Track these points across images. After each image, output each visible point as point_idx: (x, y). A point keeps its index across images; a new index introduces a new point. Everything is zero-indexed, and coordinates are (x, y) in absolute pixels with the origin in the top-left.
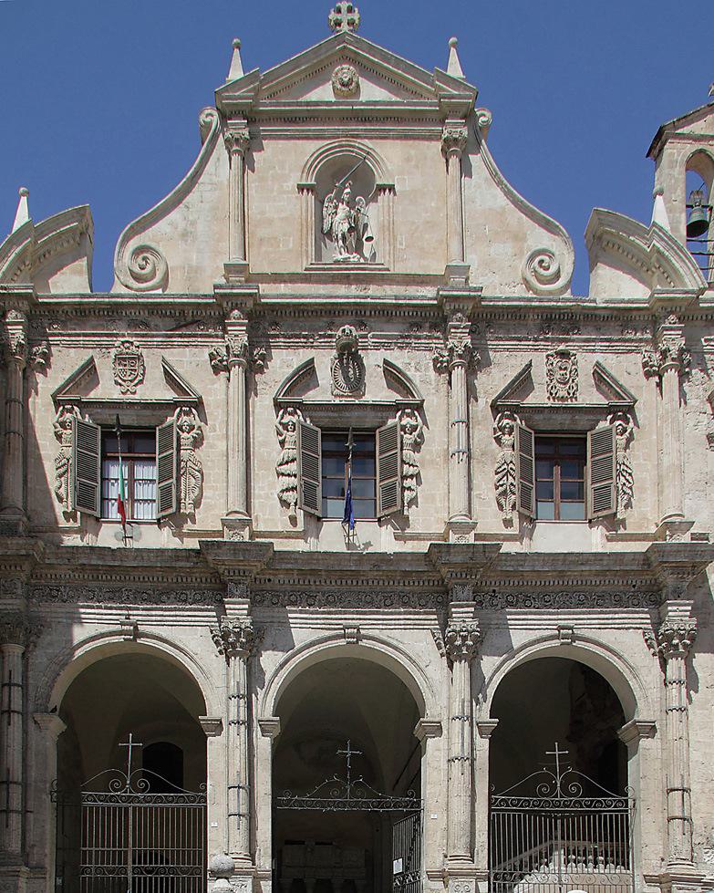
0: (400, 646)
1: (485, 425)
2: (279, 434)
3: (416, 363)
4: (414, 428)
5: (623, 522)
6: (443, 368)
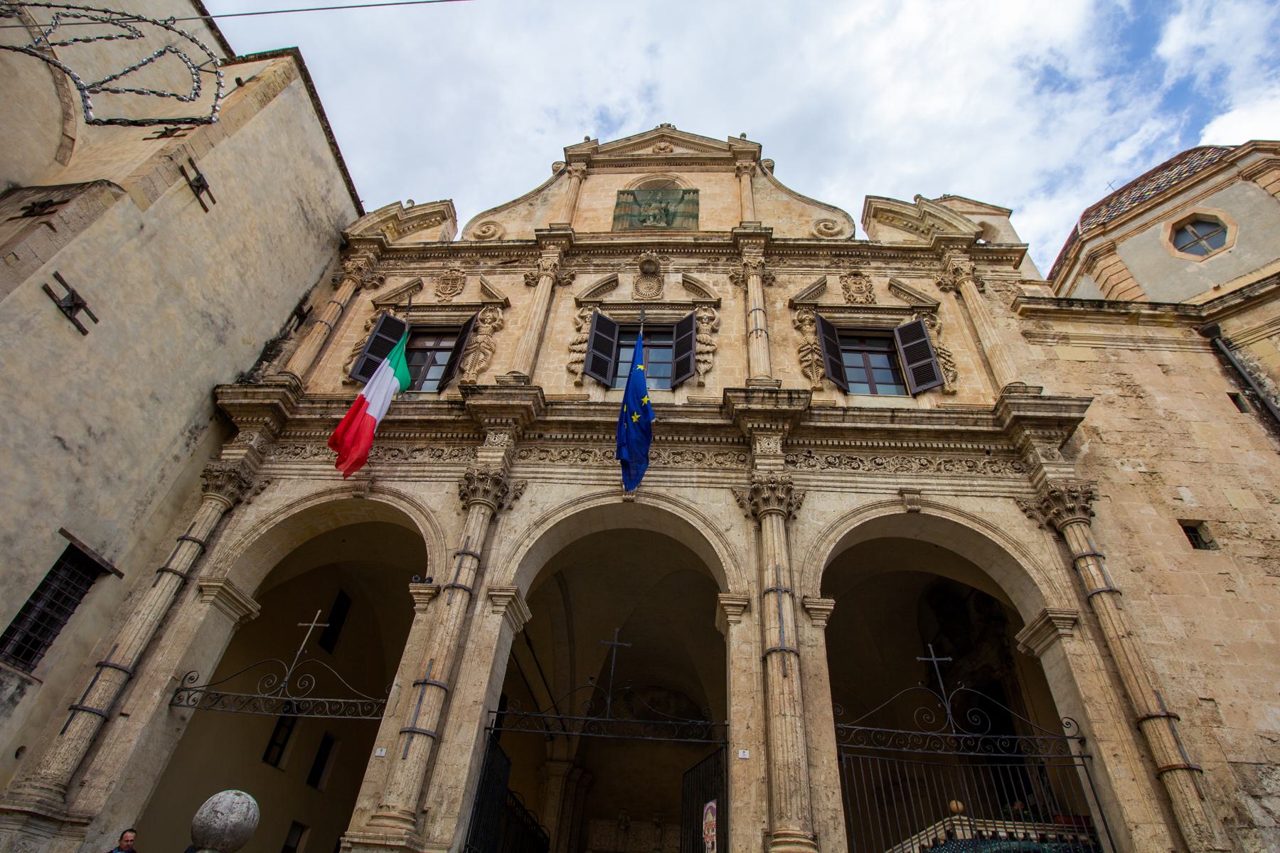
0: (693, 505)
1: (784, 324)
2: (577, 324)
3: (716, 281)
4: (712, 319)
5: (954, 393)
6: (740, 281)
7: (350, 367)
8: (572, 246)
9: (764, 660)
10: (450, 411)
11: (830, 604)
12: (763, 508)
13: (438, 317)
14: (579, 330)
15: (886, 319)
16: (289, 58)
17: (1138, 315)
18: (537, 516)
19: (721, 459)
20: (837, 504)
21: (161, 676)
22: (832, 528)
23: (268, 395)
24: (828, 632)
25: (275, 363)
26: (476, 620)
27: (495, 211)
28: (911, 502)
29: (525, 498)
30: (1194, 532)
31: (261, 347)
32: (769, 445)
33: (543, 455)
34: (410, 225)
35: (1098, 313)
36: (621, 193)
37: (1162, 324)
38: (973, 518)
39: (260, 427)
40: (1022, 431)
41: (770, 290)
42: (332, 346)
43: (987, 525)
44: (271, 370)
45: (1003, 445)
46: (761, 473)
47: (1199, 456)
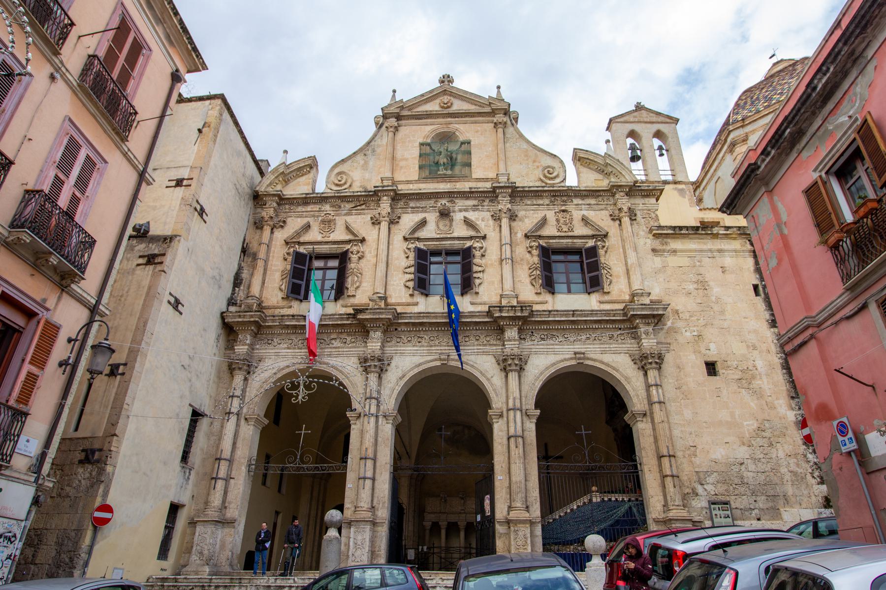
4: (482, 248)
6: (496, 218)
7: (283, 287)
8: (396, 194)
9: (509, 439)
10: (348, 319)
11: (538, 412)
12: (508, 368)
13: (324, 249)
14: (407, 257)
15: (579, 242)
16: (219, 102)
17: (718, 234)
18: (400, 374)
19: (488, 339)
20: (546, 359)
21: (242, 460)
22: (541, 373)
23: (252, 316)
24: (537, 424)
25: (242, 288)
26: (380, 427)
27: (343, 161)
28: (579, 359)
29: (393, 364)
30: (711, 368)
31: (232, 279)
32: (511, 333)
33: (398, 340)
34: (291, 175)
35: (696, 234)
36: (422, 144)
37: (731, 238)
38: (608, 365)
39: (249, 332)
40: (638, 319)
41: (514, 224)
42: (268, 272)
43: (614, 369)
44: (241, 294)
45: (627, 325)
46: (508, 351)
47: (726, 325)
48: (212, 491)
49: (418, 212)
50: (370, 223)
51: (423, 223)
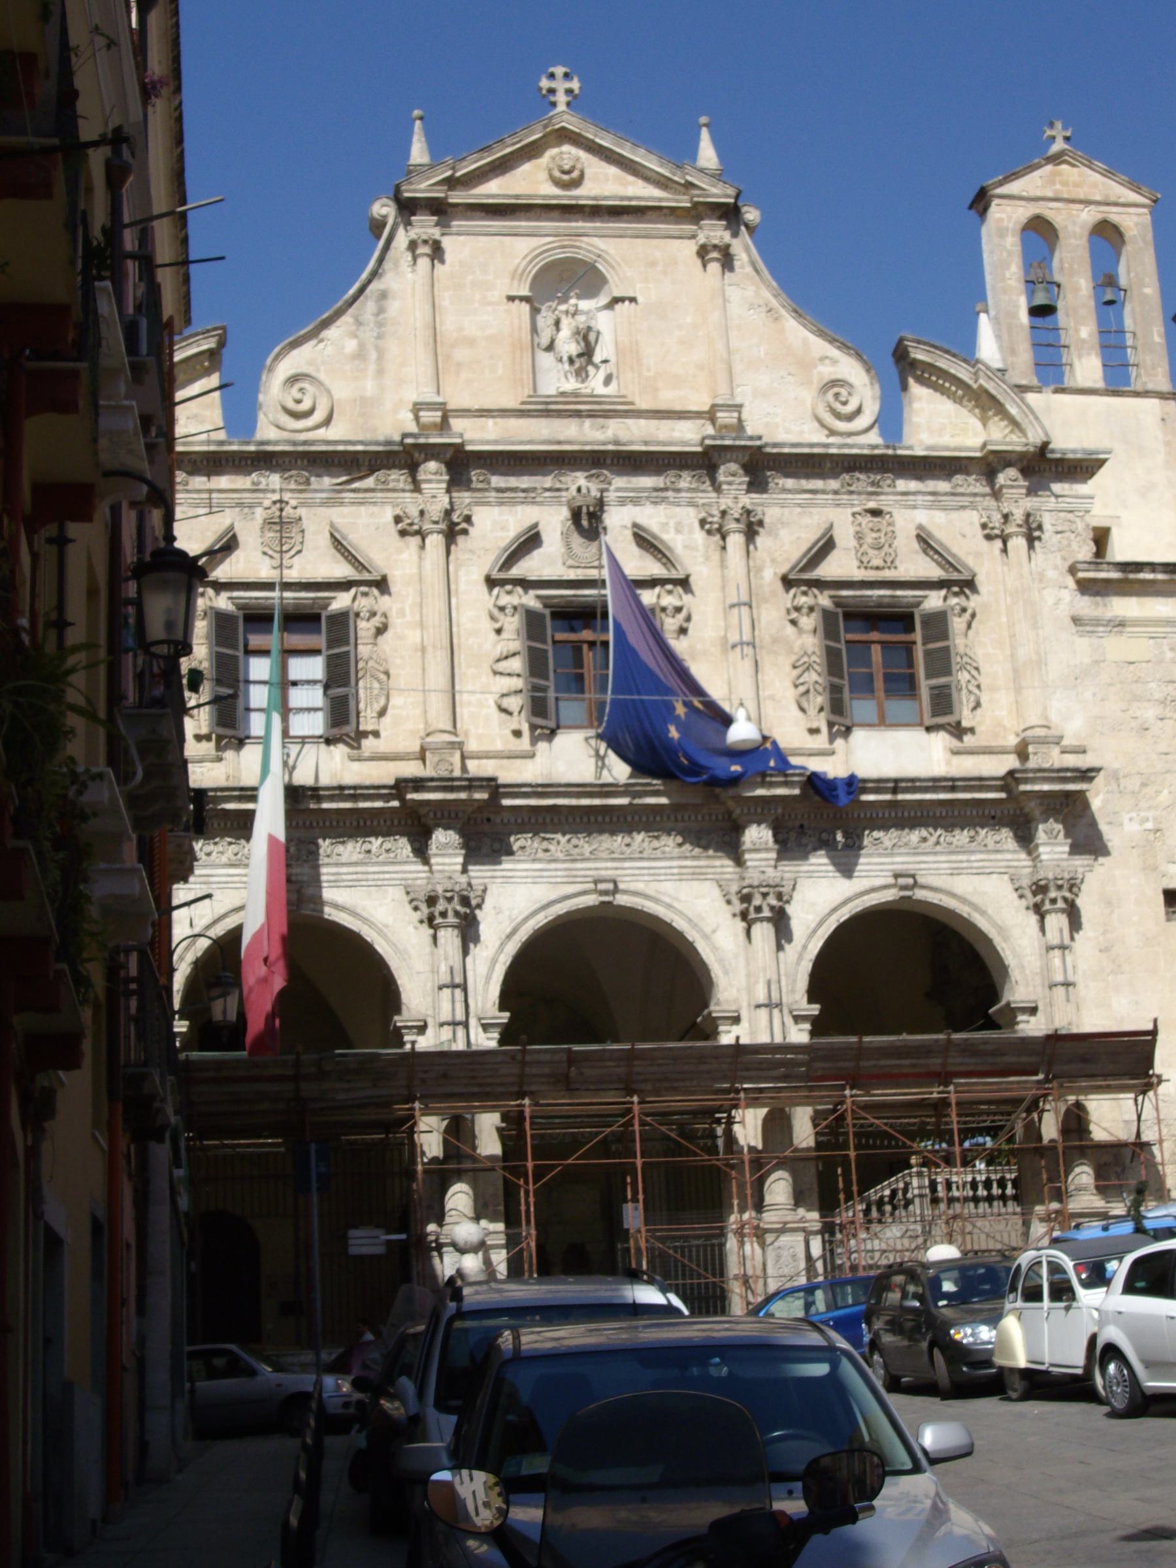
4: (678, 610)
14: (499, 631)
48: (101, 1214)
49: (513, 503)
50: (393, 530)
51: (530, 541)
